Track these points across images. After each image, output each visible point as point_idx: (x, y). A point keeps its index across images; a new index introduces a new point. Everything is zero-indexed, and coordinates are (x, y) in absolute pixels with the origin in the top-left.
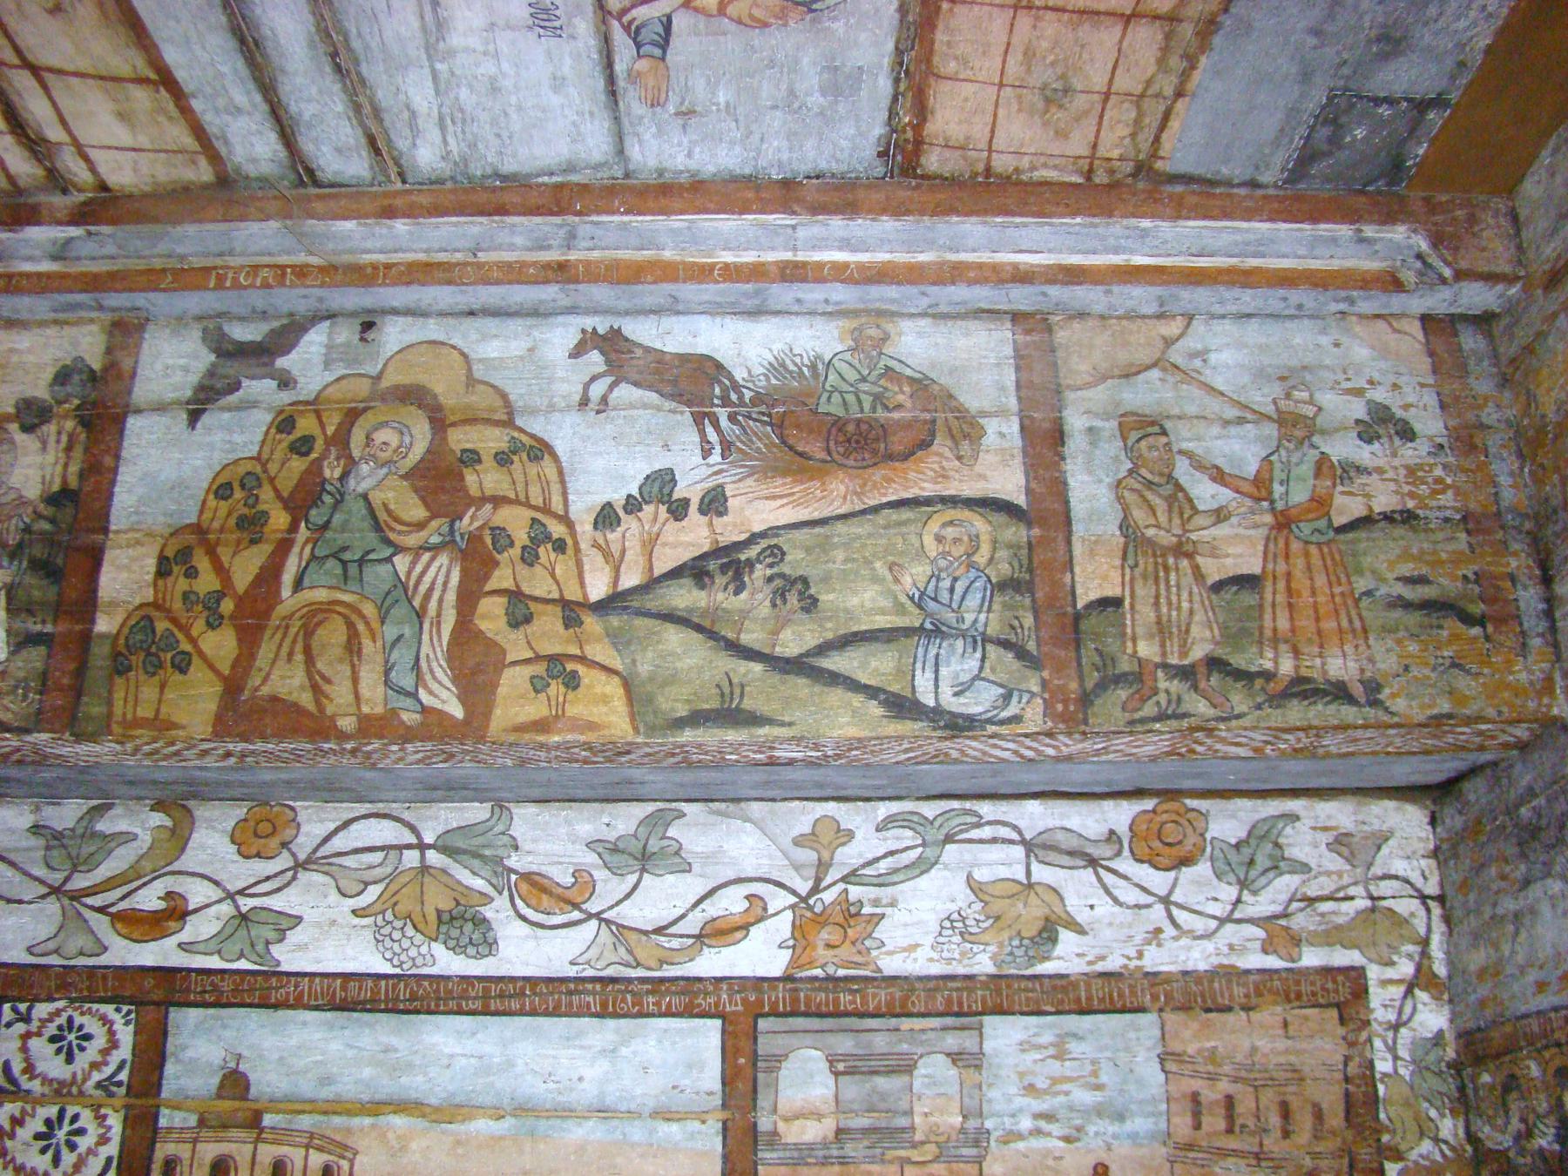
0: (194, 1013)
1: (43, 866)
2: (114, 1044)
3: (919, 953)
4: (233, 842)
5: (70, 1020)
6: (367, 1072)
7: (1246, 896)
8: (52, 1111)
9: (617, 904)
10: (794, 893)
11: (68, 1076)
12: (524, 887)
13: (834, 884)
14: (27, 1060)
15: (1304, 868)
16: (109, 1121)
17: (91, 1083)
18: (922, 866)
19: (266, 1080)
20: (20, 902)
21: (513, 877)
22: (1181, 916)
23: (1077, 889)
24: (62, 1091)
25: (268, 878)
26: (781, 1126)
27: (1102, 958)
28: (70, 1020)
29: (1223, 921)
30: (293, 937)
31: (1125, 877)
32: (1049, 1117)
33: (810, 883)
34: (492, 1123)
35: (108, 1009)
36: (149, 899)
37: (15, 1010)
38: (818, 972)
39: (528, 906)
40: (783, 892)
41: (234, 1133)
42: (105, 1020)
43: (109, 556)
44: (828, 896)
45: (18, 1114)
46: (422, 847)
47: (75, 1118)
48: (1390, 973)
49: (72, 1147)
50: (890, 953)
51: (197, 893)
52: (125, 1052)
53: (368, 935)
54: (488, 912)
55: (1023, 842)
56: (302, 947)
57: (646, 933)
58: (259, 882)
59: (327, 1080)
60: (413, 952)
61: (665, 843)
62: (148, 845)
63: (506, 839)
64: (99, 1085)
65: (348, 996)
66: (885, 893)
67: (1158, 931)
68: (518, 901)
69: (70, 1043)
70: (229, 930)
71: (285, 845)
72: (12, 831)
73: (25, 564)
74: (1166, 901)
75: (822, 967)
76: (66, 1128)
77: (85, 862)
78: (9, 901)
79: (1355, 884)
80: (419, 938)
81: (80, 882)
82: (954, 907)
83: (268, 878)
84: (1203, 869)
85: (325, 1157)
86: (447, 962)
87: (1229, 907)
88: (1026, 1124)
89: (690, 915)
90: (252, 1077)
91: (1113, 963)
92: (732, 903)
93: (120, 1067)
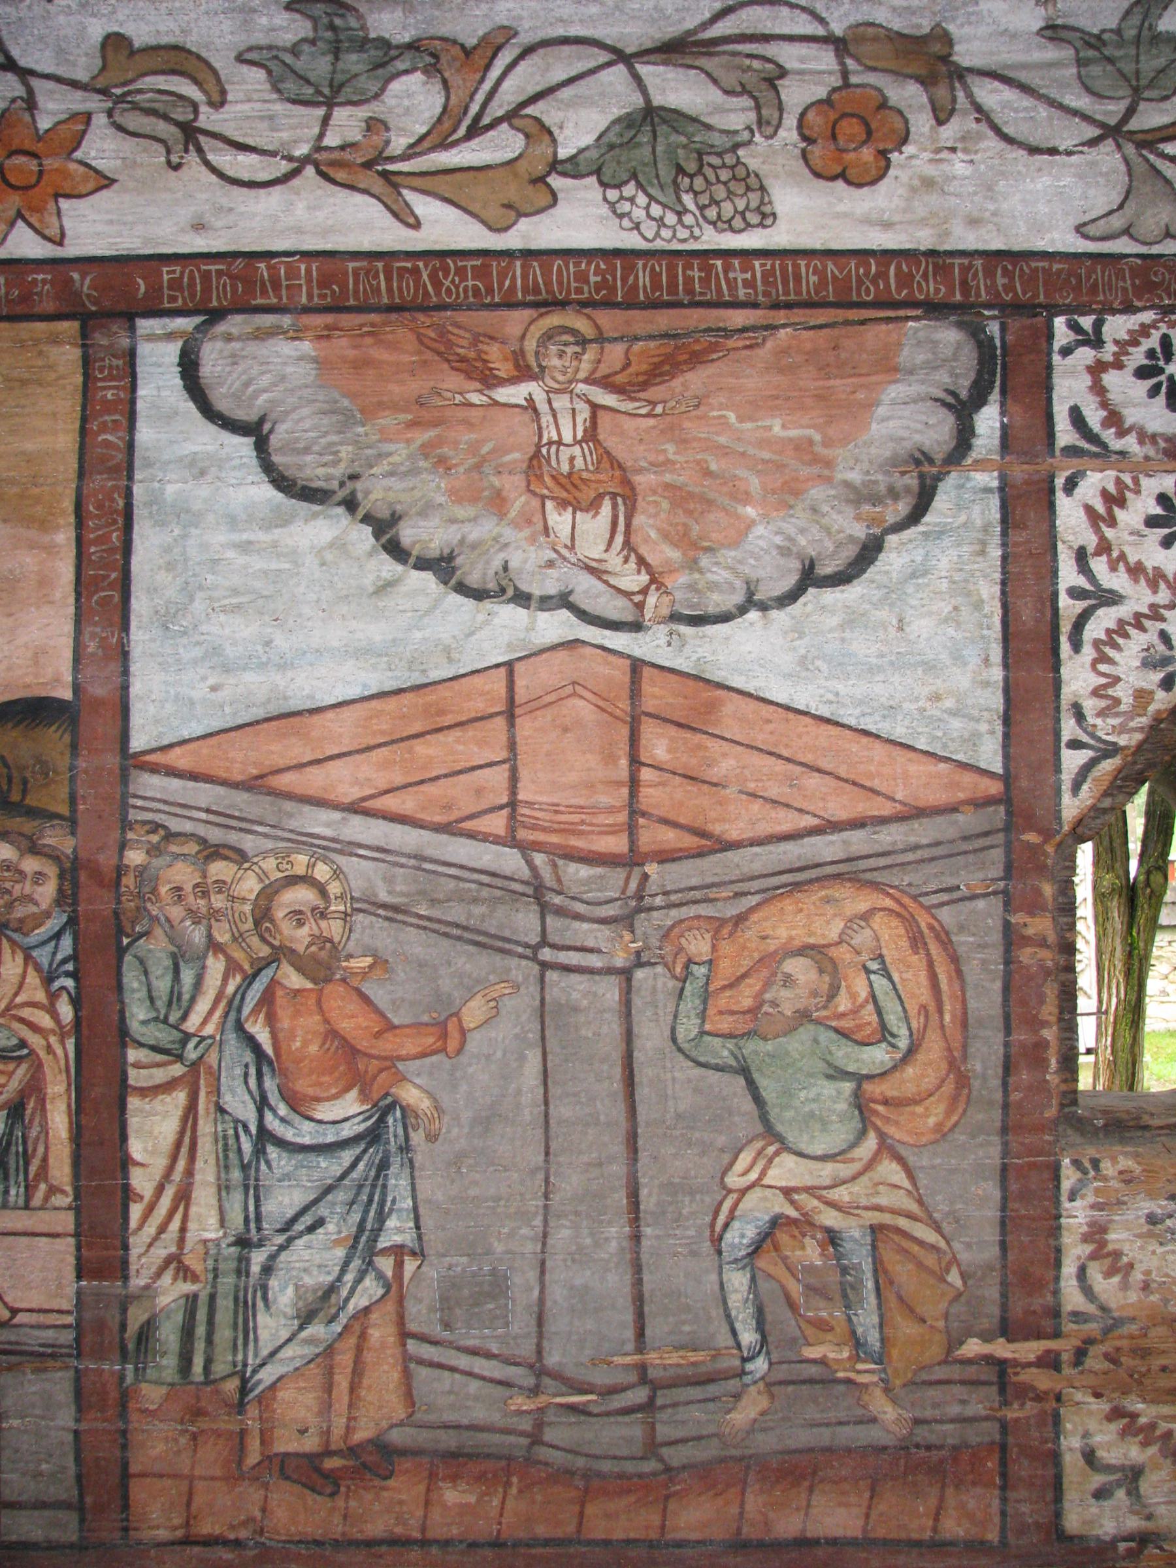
1: (1077, 88)
14: (1104, 405)
37: (1074, 327)
45: (1112, 488)
72: (1014, 36)
77: (1149, 86)
78: (1034, 150)
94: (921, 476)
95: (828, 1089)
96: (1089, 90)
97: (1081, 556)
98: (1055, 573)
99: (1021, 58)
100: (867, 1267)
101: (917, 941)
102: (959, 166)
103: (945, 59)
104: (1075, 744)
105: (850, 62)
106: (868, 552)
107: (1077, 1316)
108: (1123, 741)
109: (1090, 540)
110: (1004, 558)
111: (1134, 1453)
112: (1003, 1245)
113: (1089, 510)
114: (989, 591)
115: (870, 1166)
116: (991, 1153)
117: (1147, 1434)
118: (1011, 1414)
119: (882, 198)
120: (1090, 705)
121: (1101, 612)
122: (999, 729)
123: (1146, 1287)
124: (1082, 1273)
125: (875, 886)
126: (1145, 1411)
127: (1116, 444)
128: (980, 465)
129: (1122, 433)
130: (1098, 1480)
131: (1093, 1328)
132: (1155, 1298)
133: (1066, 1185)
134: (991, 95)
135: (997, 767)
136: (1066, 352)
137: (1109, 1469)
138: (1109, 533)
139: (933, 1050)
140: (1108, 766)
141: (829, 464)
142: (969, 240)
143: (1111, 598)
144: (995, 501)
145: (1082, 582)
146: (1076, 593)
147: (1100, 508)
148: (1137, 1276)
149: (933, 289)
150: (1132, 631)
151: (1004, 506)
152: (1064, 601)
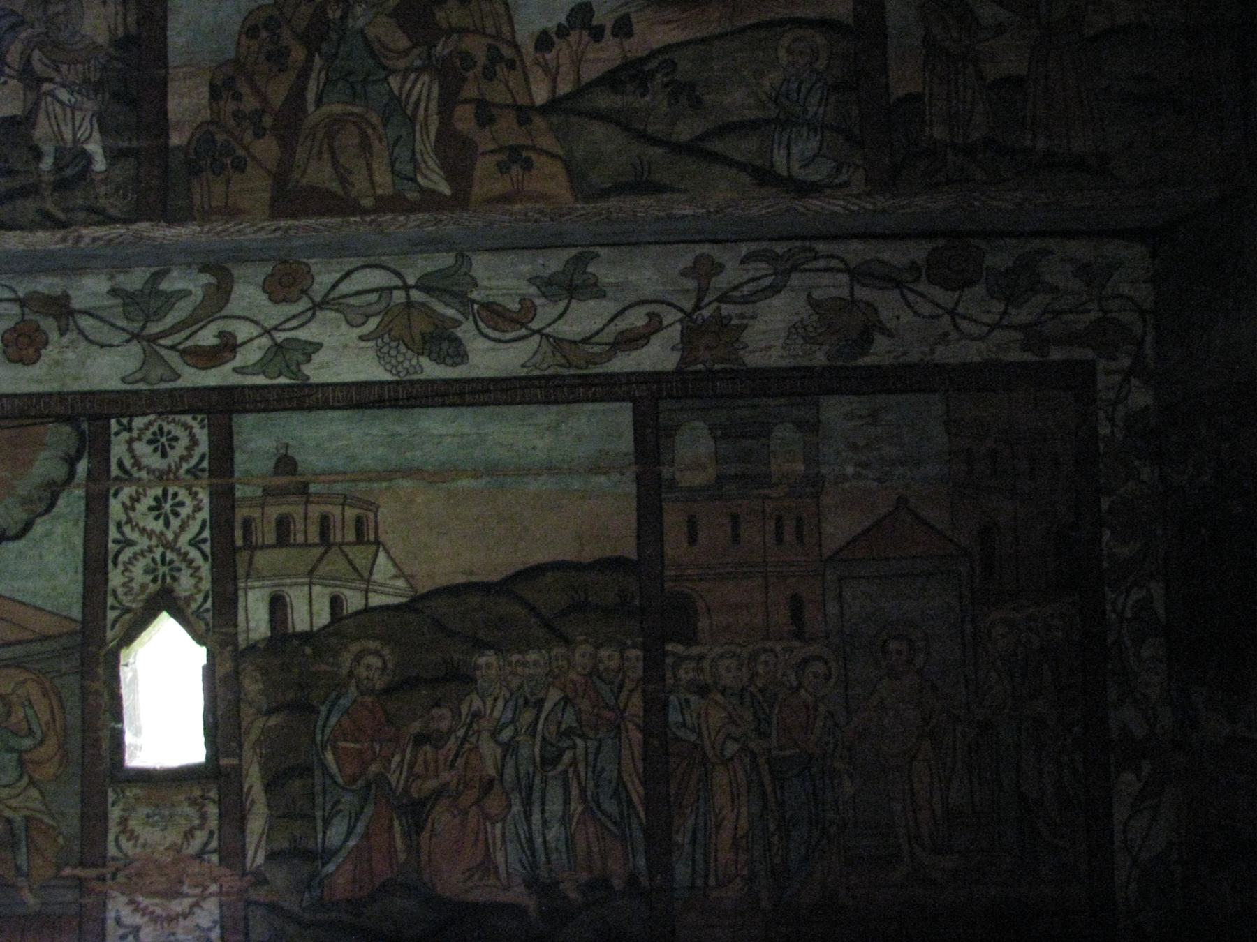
0: (250, 419)
2: (194, 442)
3: (773, 352)
4: (264, 290)
5: (161, 428)
6: (380, 451)
7: (1012, 311)
8: (159, 491)
9: (554, 322)
10: (682, 310)
11: (165, 466)
12: (484, 314)
13: (710, 303)
14: (134, 457)
15: (1054, 289)
16: (201, 496)
17: (182, 471)
18: (775, 290)
19: (309, 460)
20: (111, 346)
21: (476, 306)
22: (964, 325)
23: (888, 305)
24: (162, 476)
25: (294, 317)
26: (678, 475)
27: (905, 353)
28: (161, 428)
29: (992, 328)
30: (317, 358)
31: (922, 295)
32: (866, 465)
33: (693, 302)
34: (472, 481)
35: (188, 419)
36: (207, 337)
37: (119, 423)
38: (701, 366)
39: (489, 326)
40: (675, 311)
41: (291, 499)
42: (186, 426)
43: (173, 87)
44: (706, 313)
45: (134, 495)
46: (406, 288)
47: (175, 495)
48: (1113, 365)
49: (177, 515)
50: (754, 352)
51: (243, 331)
52: (203, 448)
53: (372, 354)
54: (459, 333)
55: (848, 270)
56: (322, 366)
57: (575, 342)
58: (288, 320)
59: (352, 458)
60: (406, 364)
61: (585, 276)
62: (199, 299)
63: (468, 278)
64: (188, 472)
65: (359, 398)
66: (748, 310)
67: (946, 334)
68: (482, 325)
69: (163, 445)
70: (270, 356)
71: (304, 292)
72: (95, 294)
73: (107, 96)
74: (952, 313)
75: (703, 363)
76: (170, 502)
77: (155, 313)
78: (102, 346)
79: (1091, 300)
80: (410, 354)
81: (154, 328)
82: (797, 319)
83: (294, 317)
84: (979, 290)
85: (356, 511)
86: (432, 370)
87: (997, 317)
88: (850, 470)
89: (606, 330)
90: (298, 458)
91: (914, 357)
92: (637, 319)
93: (202, 458)
94: (52, 493)
95: (9, 756)
96: (128, 319)
97: (119, 526)
98: (106, 533)
99: (98, 304)
100: (23, 836)
101: (45, 694)
102: (70, 355)
103: (66, 306)
104: (113, 608)
105: (26, 310)
106: (27, 527)
107: (113, 858)
108: (134, 606)
109: (123, 518)
110: (86, 529)
111: (137, 920)
112: (82, 827)
113: (123, 504)
114: (78, 541)
115: (25, 789)
116: (77, 787)
117: (144, 912)
118: (84, 901)
119: (37, 370)
120: (120, 591)
121: (127, 549)
122: (81, 601)
123: (144, 846)
124: (117, 839)
125: (27, 670)
126: (144, 901)
127: (136, 475)
128: (78, 486)
129: (140, 469)
130: (121, 931)
131: (120, 864)
132: (148, 850)
133: (110, 801)
134: (85, 322)
135: (79, 617)
136: (117, 434)
137: (126, 927)
138: (132, 514)
139: (52, 742)
140: (127, 617)
141: (14, 488)
142: (76, 387)
143: (131, 543)
144: (83, 503)
145: (118, 536)
146: (115, 541)
147: (128, 503)
148: (141, 840)
149: (60, 409)
150: (140, 558)
151: (87, 505)
152: (110, 545)
